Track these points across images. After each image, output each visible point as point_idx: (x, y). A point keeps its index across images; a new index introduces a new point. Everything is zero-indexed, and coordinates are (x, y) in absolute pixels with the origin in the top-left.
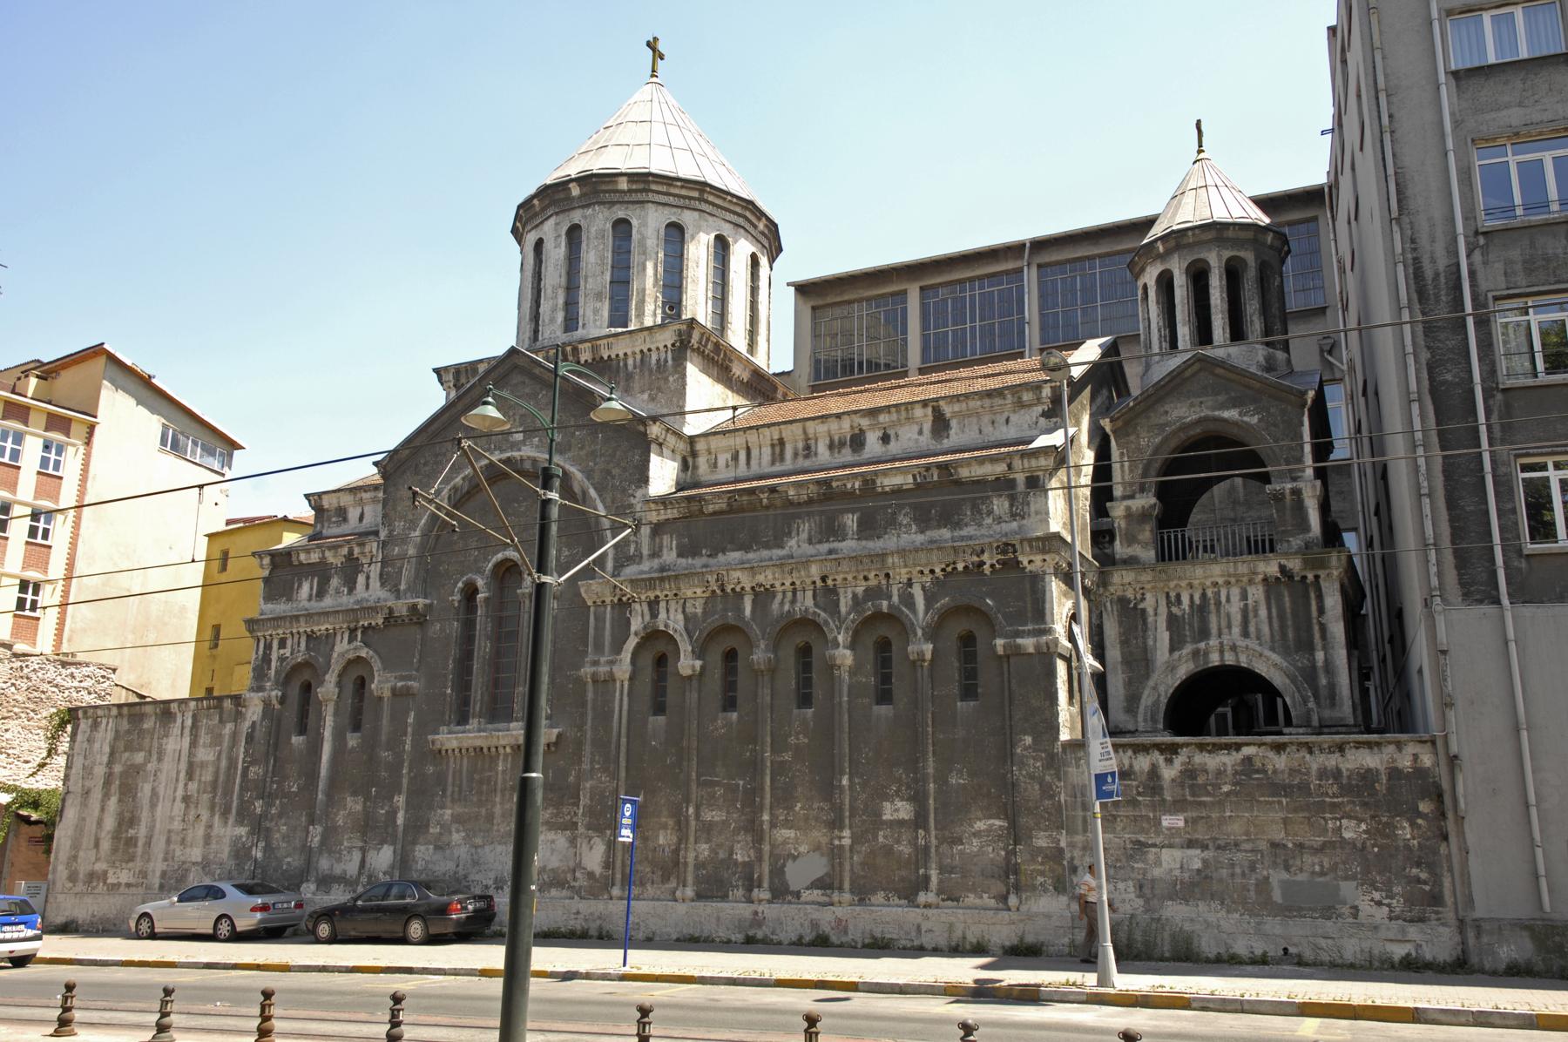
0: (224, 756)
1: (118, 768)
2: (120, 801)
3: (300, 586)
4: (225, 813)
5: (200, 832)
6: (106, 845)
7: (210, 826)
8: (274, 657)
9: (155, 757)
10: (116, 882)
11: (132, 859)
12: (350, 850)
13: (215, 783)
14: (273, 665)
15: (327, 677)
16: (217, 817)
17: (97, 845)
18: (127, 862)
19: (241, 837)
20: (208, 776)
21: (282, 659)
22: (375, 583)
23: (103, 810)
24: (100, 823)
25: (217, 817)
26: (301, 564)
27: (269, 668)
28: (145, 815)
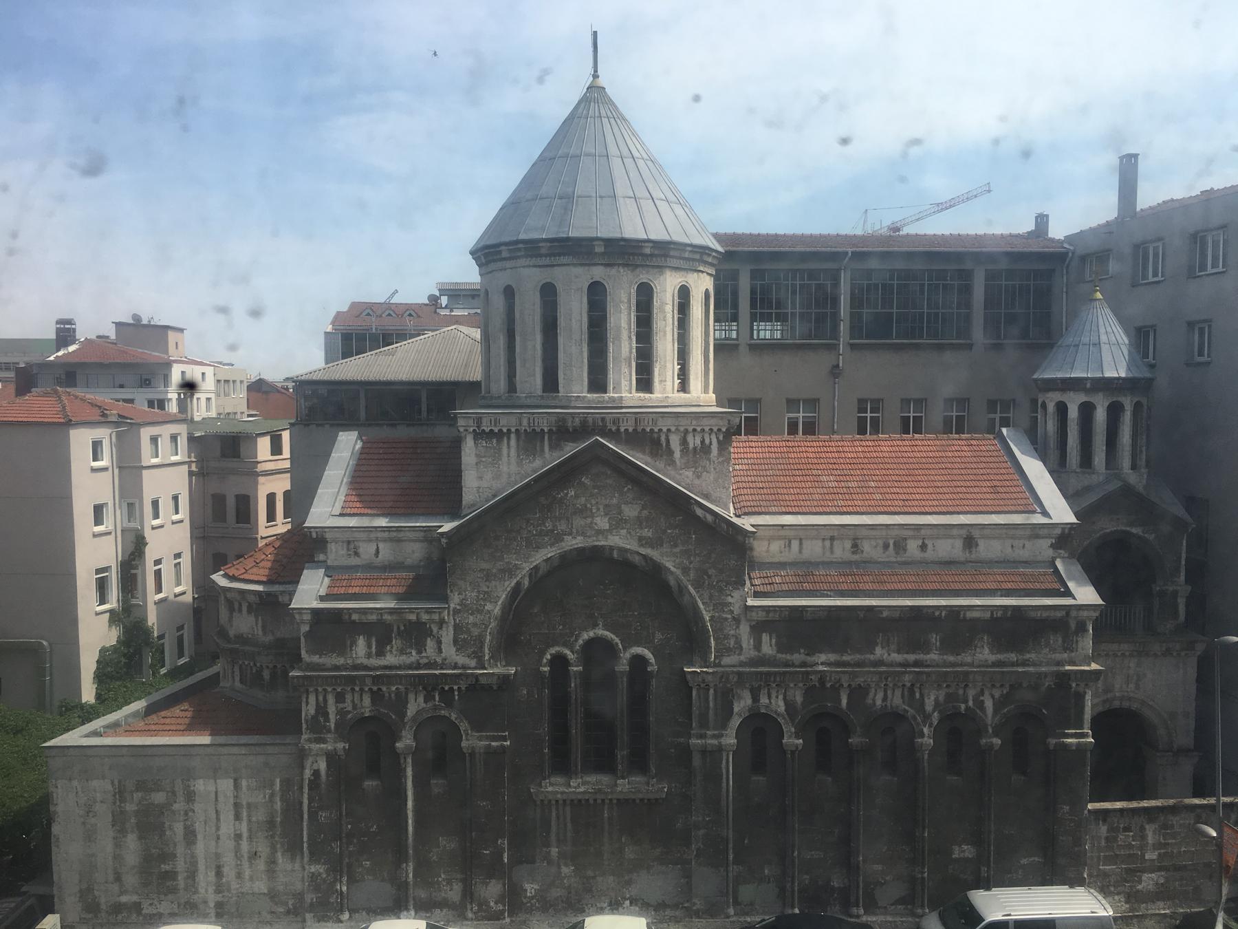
0: (278, 799)
1: (130, 807)
2: (140, 838)
3: (354, 643)
4: (293, 849)
5: (261, 865)
6: (131, 880)
7: (272, 862)
8: (332, 709)
9: (181, 798)
10: (155, 912)
11: (174, 890)
12: (449, 882)
13: (271, 823)
14: (332, 717)
15: (404, 733)
16: (279, 854)
17: (118, 878)
18: (166, 895)
19: (320, 874)
20: (260, 816)
21: (341, 713)
22: (449, 651)
23: (118, 845)
24: (117, 858)
25: (279, 854)
26: (354, 622)
27: (327, 719)
28: (180, 850)
